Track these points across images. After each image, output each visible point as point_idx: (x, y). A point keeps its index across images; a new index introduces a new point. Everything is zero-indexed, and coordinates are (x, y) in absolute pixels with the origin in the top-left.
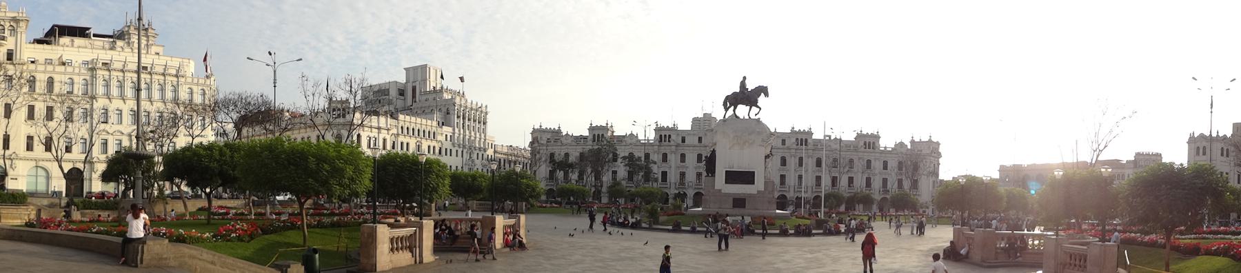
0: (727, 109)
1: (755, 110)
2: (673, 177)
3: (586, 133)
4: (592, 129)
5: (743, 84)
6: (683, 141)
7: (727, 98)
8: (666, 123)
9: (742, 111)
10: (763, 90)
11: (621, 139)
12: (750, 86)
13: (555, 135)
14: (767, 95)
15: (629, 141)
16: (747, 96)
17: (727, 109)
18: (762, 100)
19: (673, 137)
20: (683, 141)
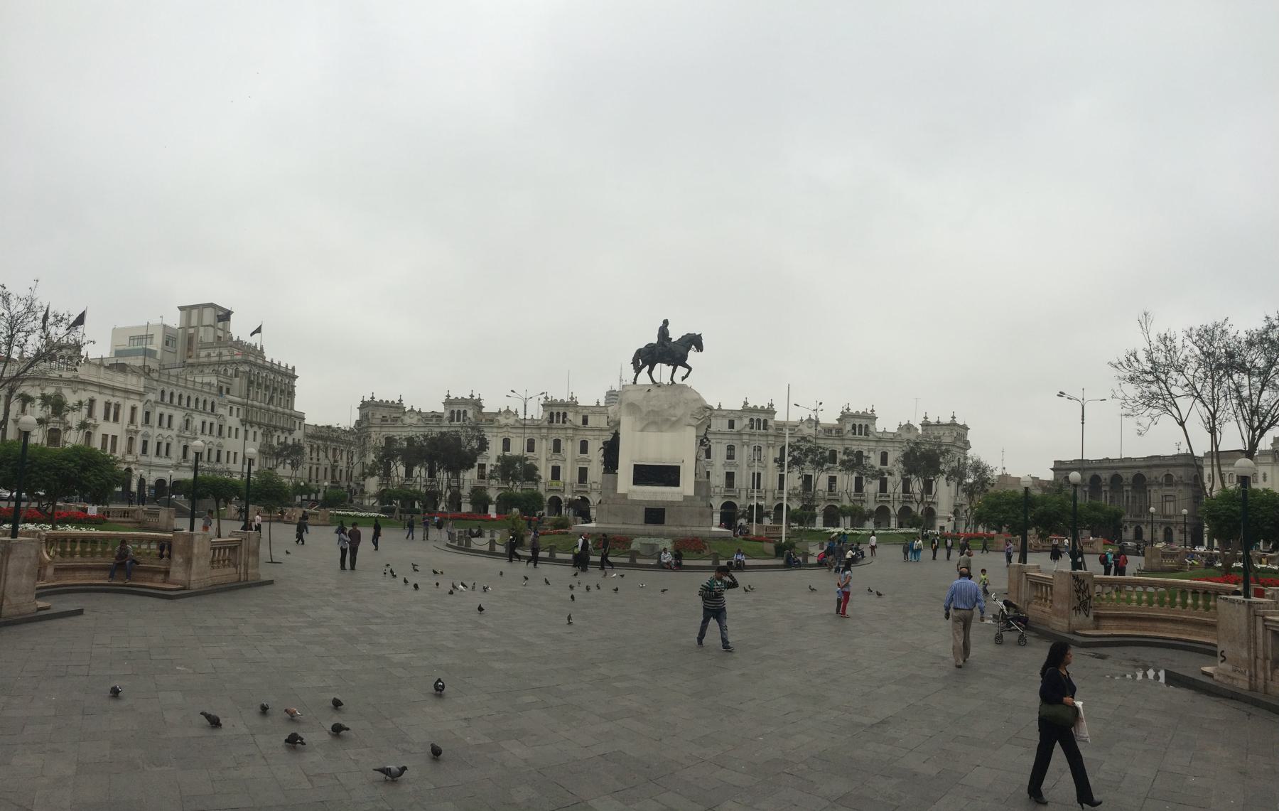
0: (638, 370)
1: (681, 371)
2: (569, 474)
3: (440, 409)
4: (449, 402)
5: (663, 332)
6: (585, 421)
7: (639, 353)
8: (560, 395)
9: (662, 372)
10: (694, 341)
11: (492, 419)
12: (675, 334)
13: (394, 411)
14: (700, 348)
15: (502, 420)
16: (668, 350)
17: (638, 370)
18: (693, 357)
19: (570, 416)
20: (585, 421)
